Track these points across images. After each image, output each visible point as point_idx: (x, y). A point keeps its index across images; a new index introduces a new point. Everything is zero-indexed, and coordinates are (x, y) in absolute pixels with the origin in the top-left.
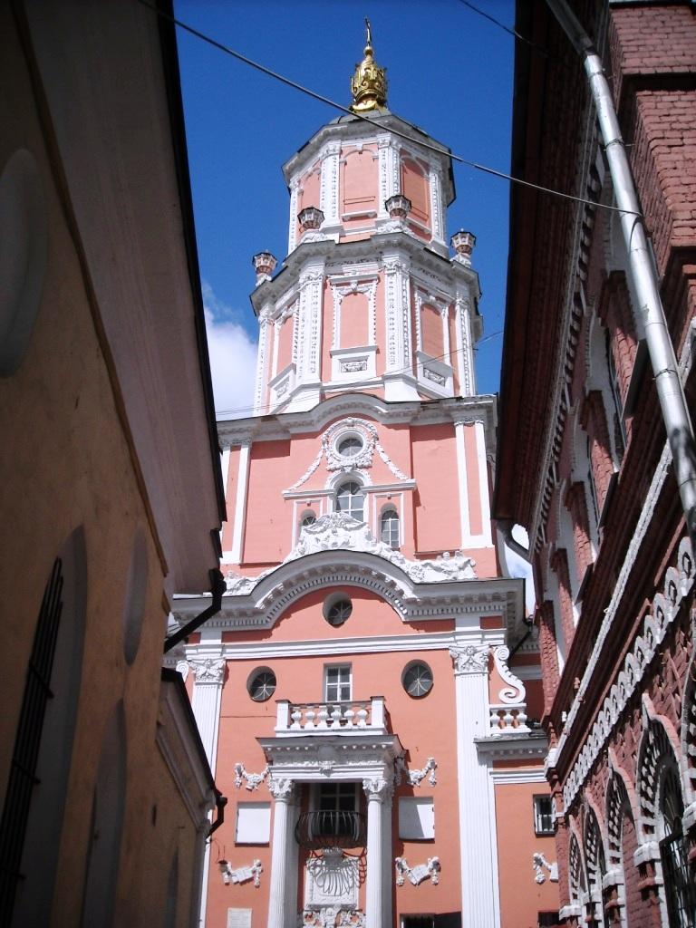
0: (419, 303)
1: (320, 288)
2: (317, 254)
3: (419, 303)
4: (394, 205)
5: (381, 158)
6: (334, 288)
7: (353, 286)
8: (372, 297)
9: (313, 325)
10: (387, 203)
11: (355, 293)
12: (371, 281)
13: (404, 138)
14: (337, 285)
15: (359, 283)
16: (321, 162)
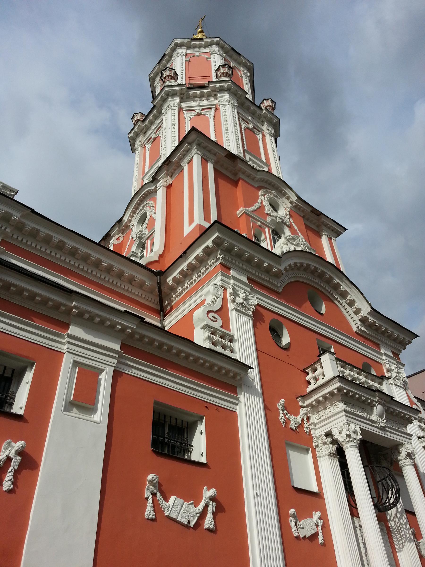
0: (243, 127)
1: (176, 112)
2: (174, 94)
3: (243, 127)
4: (222, 70)
5: (212, 60)
6: (185, 112)
7: (197, 111)
8: (212, 117)
9: (173, 130)
10: (218, 70)
11: (199, 114)
12: (211, 108)
13: (226, 53)
14: (188, 111)
15: (203, 109)
16: (172, 64)
